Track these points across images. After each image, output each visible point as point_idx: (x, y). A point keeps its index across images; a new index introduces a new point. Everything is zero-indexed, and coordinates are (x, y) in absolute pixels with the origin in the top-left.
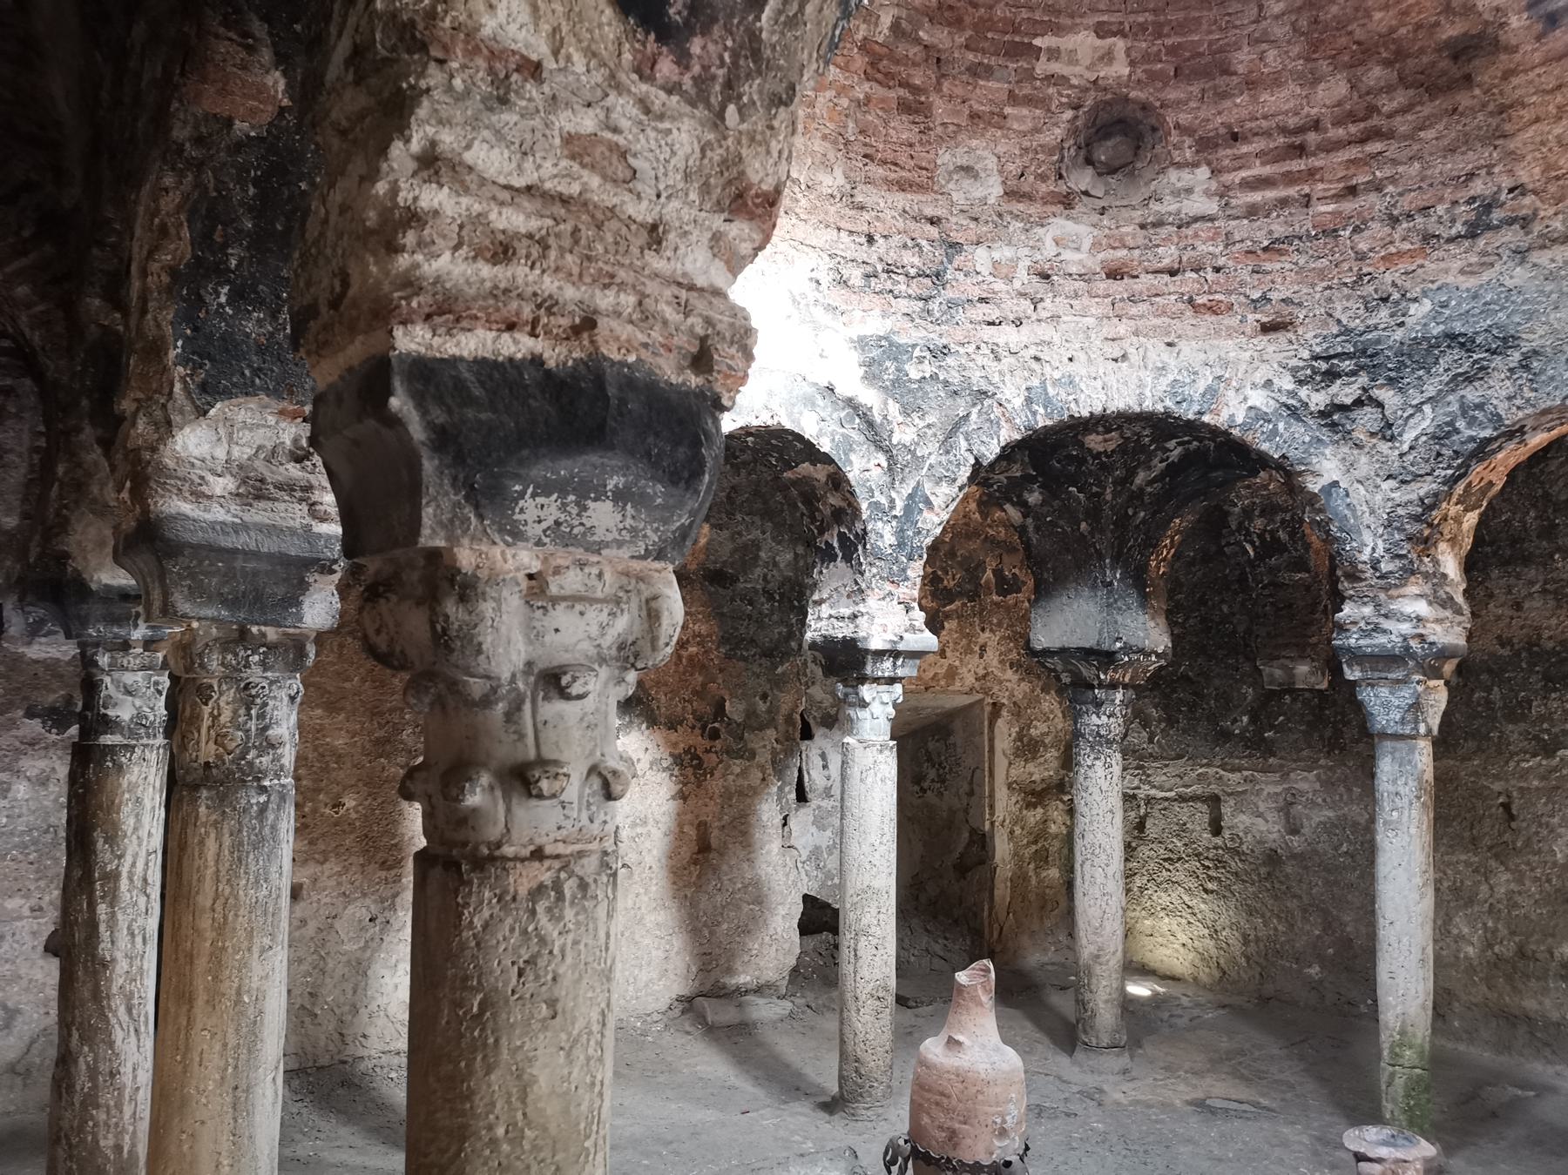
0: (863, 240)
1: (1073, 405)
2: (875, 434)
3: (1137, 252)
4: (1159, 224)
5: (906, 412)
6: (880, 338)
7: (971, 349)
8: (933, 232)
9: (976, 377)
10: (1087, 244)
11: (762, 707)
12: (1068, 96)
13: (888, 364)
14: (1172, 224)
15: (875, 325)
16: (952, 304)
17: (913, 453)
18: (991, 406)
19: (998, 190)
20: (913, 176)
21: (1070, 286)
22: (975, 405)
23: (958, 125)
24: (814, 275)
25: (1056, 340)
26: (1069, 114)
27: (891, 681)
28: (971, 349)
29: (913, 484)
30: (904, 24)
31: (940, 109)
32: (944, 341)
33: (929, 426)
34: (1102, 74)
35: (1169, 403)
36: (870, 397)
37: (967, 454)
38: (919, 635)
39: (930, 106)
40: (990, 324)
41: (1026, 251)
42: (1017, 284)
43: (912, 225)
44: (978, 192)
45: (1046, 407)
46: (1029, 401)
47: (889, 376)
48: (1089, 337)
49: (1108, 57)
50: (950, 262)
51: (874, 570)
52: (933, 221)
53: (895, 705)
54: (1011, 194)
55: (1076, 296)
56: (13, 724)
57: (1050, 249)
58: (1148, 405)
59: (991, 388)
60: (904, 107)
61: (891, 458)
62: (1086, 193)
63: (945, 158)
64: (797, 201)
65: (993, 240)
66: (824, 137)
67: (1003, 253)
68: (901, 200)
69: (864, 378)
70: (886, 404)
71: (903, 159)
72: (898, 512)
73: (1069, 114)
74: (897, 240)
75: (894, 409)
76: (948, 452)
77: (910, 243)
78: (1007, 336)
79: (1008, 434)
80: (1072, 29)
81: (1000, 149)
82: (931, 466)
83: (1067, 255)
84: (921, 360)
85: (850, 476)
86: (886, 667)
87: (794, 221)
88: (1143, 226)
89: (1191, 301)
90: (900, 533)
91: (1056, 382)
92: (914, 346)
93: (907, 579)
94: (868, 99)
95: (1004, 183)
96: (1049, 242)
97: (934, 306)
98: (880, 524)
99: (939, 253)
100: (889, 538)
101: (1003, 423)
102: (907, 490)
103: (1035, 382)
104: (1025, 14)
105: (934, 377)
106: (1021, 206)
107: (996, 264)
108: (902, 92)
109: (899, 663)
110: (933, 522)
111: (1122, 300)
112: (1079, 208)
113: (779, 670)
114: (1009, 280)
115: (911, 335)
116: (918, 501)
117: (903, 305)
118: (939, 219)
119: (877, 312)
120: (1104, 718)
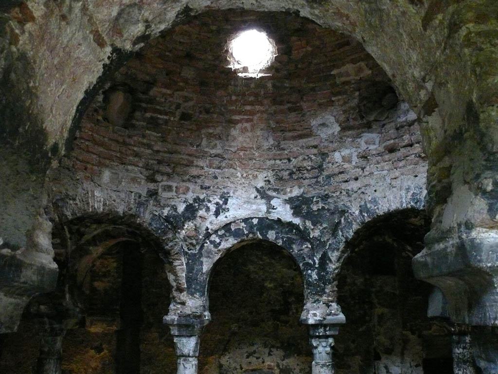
0: (286, 161)
1: (377, 211)
2: (303, 235)
3: (397, 140)
4: (402, 127)
5: (314, 224)
6: (298, 197)
7: (338, 193)
8: (315, 151)
9: (340, 204)
10: (377, 142)
11: (352, 346)
12: (353, 88)
13: (303, 206)
14: (406, 125)
15: (296, 192)
16: (329, 177)
17: (320, 240)
18: (348, 216)
19: (338, 129)
20: (305, 132)
21: (374, 160)
22: (341, 217)
23: (314, 110)
24: (267, 179)
25: (372, 182)
26: (357, 93)
27: (327, 337)
28: (338, 193)
29: (321, 253)
30: (278, 84)
31: (305, 105)
32: (326, 193)
33: (325, 228)
34: (362, 76)
35: (412, 204)
36: (297, 221)
37: (342, 238)
38: (335, 317)
39: (301, 106)
40: (346, 181)
41: (354, 149)
42: (354, 163)
43: (307, 151)
44: (330, 132)
45: (367, 214)
46: (361, 212)
47: (304, 211)
48: (385, 179)
49: (360, 70)
50: (324, 160)
51: (309, 291)
52: (315, 147)
53: (332, 348)
54: (344, 129)
55: (378, 163)
56: (87, 352)
57: (364, 146)
58: (404, 205)
59: (346, 209)
60: (290, 110)
61: (311, 244)
62: (376, 120)
63: (314, 123)
64: (254, 154)
65: (340, 149)
66: (261, 129)
67: (346, 152)
68: (302, 142)
69: (293, 214)
70: (305, 222)
71: (297, 128)
72: (317, 266)
73: (357, 93)
74: (301, 158)
75: (309, 224)
76: (335, 238)
77: (306, 158)
78: (354, 185)
79: (355, 227)
80: (343, 64)
81: (335, 114)
82: (330, 245)
83: (372, 147)
84: (317, 202)
85: (293, 253)
86: (321, 331)
87: (254, 161)
88: (397, 129)
89: (420, 156)
90: (318, 274)
91: (370, 202)
92: (313, 197)
93: (325, 293)
94: (275, 112)
95: (340, 125)
96: (363, 143)
97: (320, 179)
98: (310, 271)
99: (319, 159)
100: (315, 276)
101: (354, 223)
102: (319, 256)
103: (363, 203)
104: (322, 65)
105: (323, 208)
106: (350, 132)
107: (343, 157)
108: (289, 105)
109: (328, 329)
110: (333, 267)
111: (395, 161)
112: (374, 127)
113: (361, 330)
114: (350, 162)
115: (313, 193)
116: (324, 259)
117: (306, 182)
118: (317, 146)
119: (296, 187)
120: (461, 350)
